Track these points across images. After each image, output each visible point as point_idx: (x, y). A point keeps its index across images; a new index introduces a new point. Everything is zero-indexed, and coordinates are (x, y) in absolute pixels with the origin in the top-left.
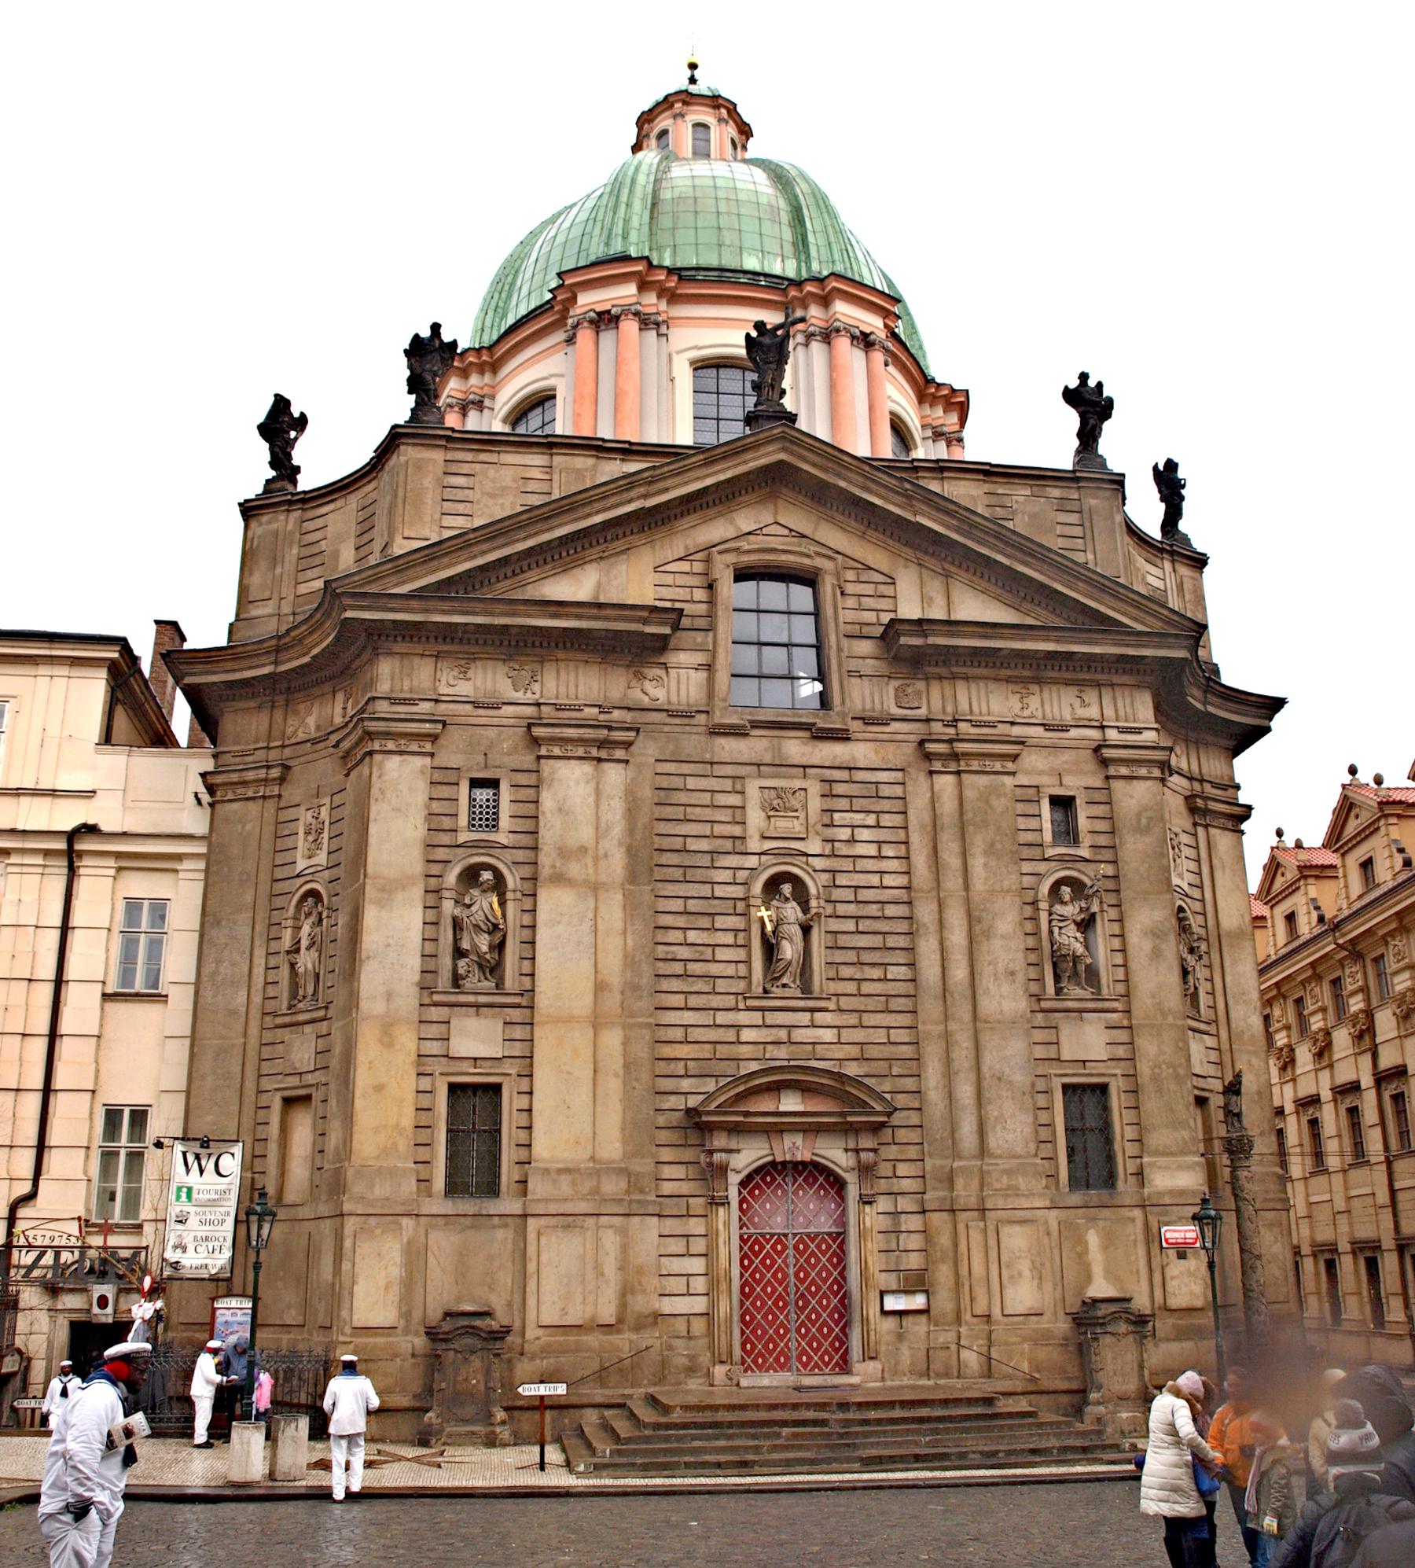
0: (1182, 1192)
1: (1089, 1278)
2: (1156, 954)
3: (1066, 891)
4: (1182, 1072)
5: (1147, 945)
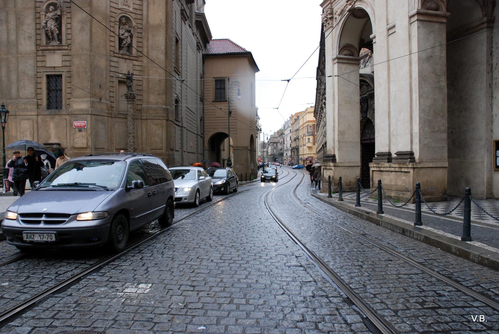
0: (82, 110)
1: (50, 138)
2: (82, 29)
3: (51, 8)
4: (87, 70)
5: (79, 26)
